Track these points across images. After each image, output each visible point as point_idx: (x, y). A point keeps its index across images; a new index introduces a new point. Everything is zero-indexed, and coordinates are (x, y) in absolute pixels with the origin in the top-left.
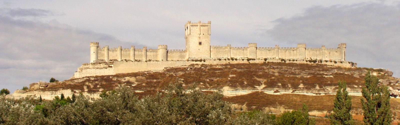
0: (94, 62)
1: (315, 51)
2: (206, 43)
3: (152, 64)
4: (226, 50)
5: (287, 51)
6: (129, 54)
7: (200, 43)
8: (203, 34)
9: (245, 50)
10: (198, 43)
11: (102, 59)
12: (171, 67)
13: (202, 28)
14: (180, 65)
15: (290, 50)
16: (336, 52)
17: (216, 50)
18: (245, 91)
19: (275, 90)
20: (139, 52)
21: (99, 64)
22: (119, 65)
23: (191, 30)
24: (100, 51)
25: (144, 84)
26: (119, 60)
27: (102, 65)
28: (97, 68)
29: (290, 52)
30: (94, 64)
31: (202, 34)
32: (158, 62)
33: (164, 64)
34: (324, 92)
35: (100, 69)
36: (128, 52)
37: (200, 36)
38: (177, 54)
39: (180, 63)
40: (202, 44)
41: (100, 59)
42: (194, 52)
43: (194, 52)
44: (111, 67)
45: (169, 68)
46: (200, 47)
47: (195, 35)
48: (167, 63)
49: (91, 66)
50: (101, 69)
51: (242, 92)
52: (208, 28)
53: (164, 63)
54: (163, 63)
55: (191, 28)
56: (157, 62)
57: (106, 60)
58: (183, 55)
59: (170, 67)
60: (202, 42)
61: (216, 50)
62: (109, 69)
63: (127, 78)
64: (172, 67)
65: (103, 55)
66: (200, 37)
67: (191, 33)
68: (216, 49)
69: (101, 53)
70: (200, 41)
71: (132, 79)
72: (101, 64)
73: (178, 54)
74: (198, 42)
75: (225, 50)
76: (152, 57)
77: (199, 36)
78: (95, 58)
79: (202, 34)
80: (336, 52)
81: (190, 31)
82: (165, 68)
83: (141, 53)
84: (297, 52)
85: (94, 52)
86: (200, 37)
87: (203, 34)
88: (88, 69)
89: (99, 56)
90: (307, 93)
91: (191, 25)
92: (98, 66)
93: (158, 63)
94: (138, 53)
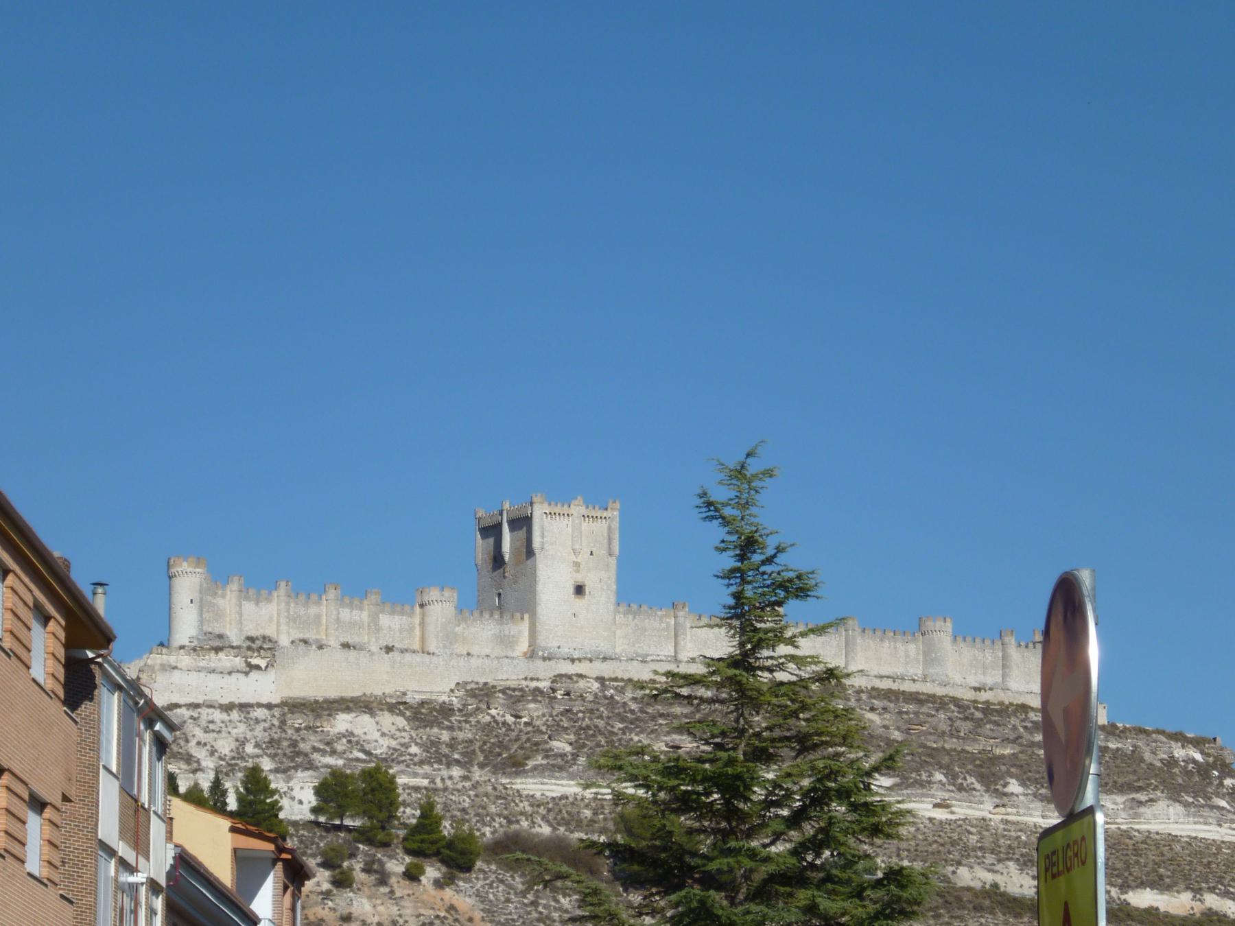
0: (193, 644)
1: (977, 649)
3: (411, 666)
6: (318, 617)
7: (579, 590)
8: (591, 553)
10: (572, 590)
11: (217, 631)
12: (482, 680)
14: (514, 677)
15: (895, 642)
17: (633, 620)
19: (938, 801)
21: (213, 654)
22: (294, 663)
23: (546, 534)
24: (209, 598)
25: (414, 749)
26: (284, 641)
27: (225, 660)
28: (213, 671)
29: (895, 648)
30: (194, 650)
32: (434, 659)
35: (221, 673)
36: (313, 610)
38: (489, 627)
40: (587, 592)
42: (557, 626)
43: (557, 626)
44: (258, 667)
45: (473, 686)
46: (580, 603)
47: (559, 554)
49: (185, 660)
50: (226, 676)
53: (453, 662)
54: (451, 664)
55: (547, 521)
57: (235, 637)
58: (507, 633)
59: (477, 683)
61: (633, 620)
62: (254, 675)
63: (342, 722)
64: (486, 684)
65: (219, 615)
67: (546, 546)
68: (631, 617)
69: (214, 604)
70: (580, 578)
71: (362, 725)
72: (221, 655)
76: (398, 634)
77: (576, 560)
81: (543, 536)
82: (458, 683)
83: (360, 616)
85: (192, 601)
88: (176, 671)
89: (206, 616)
90: (1043, 817)
92: (214, 660)
93: (431, 663)
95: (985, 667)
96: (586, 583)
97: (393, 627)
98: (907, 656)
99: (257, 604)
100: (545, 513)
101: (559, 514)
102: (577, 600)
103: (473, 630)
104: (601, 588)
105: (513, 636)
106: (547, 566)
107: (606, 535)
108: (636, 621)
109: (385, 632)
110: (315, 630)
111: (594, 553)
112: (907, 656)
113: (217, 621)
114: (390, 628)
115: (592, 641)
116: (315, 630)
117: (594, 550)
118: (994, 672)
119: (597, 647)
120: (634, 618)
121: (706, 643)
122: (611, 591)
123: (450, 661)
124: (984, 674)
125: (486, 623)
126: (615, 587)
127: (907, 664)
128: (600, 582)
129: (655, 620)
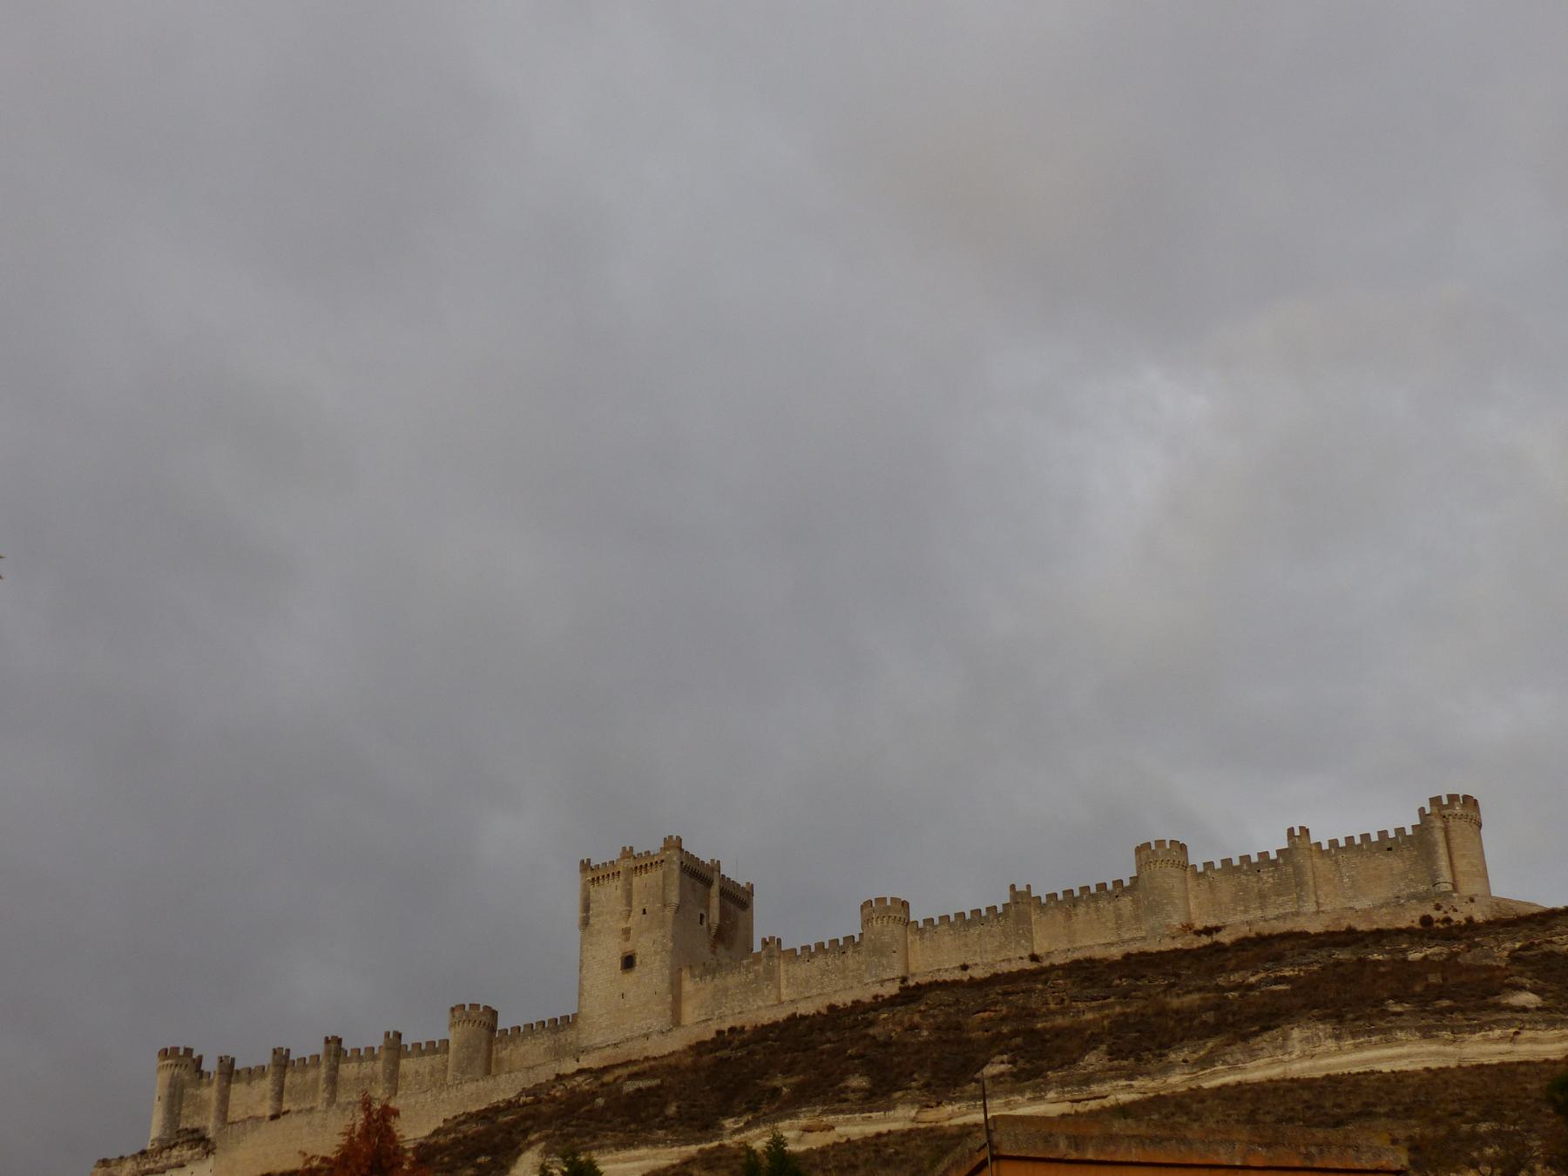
2: (656, 953)
4: (755, 971)
5: (1081, 910)
7: (628, 962)
8: (644, 911)
9: (849, 953)
10: (617, 963)
11: (196, 1125)
13: (636, 880)
16: (1390, 849)
18: (640, 1159)
20: (364, 1064)
24: (191, 1091)
29: (1097, 909)
31: (637, 910)
33: (443, 1101)
34: (1123, 1083)
37: (631, 923)
38: (541, 1041)
39: (513, 1081)
40: (638, 961)
41: (188, 1126)
42: (602, 1015)
43: (602, 1015)
48: (459, 1094)
51: (621, 1166)
52: (664, 872)
53: (444, 1095)
54: (441, 1097)
66: (627, 931)
67: (591, 921)
69: (197, 1096)
70: (628, 947)
73: (545, 1042)
74: (620, 955)
75: (751, 976)
76: (427, 1077)
77: (625, 926)
78: (161, 1123)
79: (637, 910)
80: (1390, 849)
84: (1136, 902)
86: (627, 931)
87: (644, 911)
93: (416, 1102)
94: (356, 1070)
95: (1262, 896)
96: (638, 951)
97: (421, 1071)
98: (1119, 917)
99: (249, 1084)
101: (603, 877)
102: (626, 976)
103: (523, 1049)
104: (656, 953)
105: (570, 1044)
106: (591, 945)
107: (661, 883)
109: (410, 1078)
110: (311, 1098)
111: (647, 911)
112: (1119, 917)
113: (198, 1114)
114: (417, 1072)
115: (643, 1022)
116: (311, 1098)
118: (1280, 900)
119: (649, 1028)
121: (807, 982)
122: (666, 952)
123: (440, 1093)
124: (1262, 907)
125: (538, 1036)
126: (671, 945)
127: (1119, 927)
128: (654, 944)
129: (740, 972)
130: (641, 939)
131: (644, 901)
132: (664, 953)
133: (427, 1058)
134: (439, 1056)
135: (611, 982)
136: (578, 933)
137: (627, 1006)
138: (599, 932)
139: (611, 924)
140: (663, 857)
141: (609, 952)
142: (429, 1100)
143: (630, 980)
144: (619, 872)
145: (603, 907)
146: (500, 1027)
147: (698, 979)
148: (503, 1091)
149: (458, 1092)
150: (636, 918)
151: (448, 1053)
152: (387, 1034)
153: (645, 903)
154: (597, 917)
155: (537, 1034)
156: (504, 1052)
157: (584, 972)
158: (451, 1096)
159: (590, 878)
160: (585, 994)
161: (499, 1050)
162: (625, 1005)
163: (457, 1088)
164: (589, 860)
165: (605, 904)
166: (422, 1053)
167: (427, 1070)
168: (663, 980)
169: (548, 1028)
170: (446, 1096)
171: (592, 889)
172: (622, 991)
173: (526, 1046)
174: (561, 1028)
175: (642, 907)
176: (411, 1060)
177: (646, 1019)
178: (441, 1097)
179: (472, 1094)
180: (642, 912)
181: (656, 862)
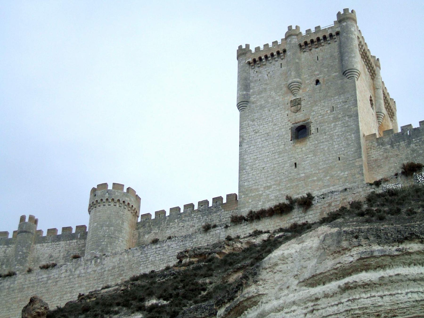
2: (336, 119)
8: (317, 82)
23: (252, 84)
38: (191, 223)
39: (165, 251)
40: (313, 129)
43: (269, 187)
53: (81, 270)
54: (77, 272)
56: (44, 275)
60: (308, 123)
67: (252, 99)
68: (402, 144)
74: (290, 125)
87: (317, 82)
91: (250, 60)
93: (49, 278)
100: (249, 63)
102: (298, 145)
107: (336, 54)
108: (412, 145)
117: (321, 78)
120: (409, 143)
125: (187, 219)
130: (315, 108)
131: (317, 73)
132: (347, 118)
133: (62, 243)
134: (75, 241)
135: (280, 153)
136: (237, 113)
137: (303, 175)
138: (262, 107)
139: (276, 98)
140: (338, 29)
141: (275, 124)
142: (63, 275)
143: (304, 149)
144: (285, 51)
145: (267, 84)
146: (143, 211)
147: (388, 146)
148: (153, 263)
149: (97, 266)
150: (308, 90)
151: (85, 239)
152: (23, 218)
153: (318, 75)
154: (259, 94)
155: (186, 216)
156: (147, 236)
157: (245, 146)
158: (89, 270)
159: (250, 60)
160: (247, 168)
161: (142, 234)
162: (299, 174)
163: (96, 262)
164: (247, 46)
165: (268, 82)
166: (58, 238)
167: (62, 254)
168: (348, 145)
169: (198, 210)
170: (83, 271)
171: (252, 73)
172: (294, 161)
173: (173, 230)
174: (215, 210)
175: (314, 79)
176: (45, 245)
177: (328, 186)
178: (77, 272)
179: (114, 268)
180: (315, 82)
181: (331, 35)
